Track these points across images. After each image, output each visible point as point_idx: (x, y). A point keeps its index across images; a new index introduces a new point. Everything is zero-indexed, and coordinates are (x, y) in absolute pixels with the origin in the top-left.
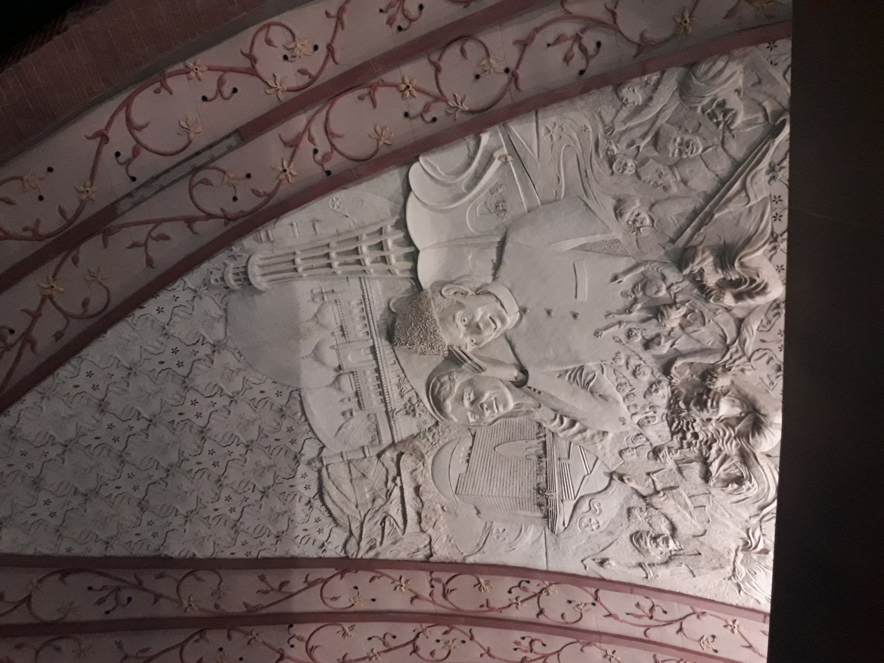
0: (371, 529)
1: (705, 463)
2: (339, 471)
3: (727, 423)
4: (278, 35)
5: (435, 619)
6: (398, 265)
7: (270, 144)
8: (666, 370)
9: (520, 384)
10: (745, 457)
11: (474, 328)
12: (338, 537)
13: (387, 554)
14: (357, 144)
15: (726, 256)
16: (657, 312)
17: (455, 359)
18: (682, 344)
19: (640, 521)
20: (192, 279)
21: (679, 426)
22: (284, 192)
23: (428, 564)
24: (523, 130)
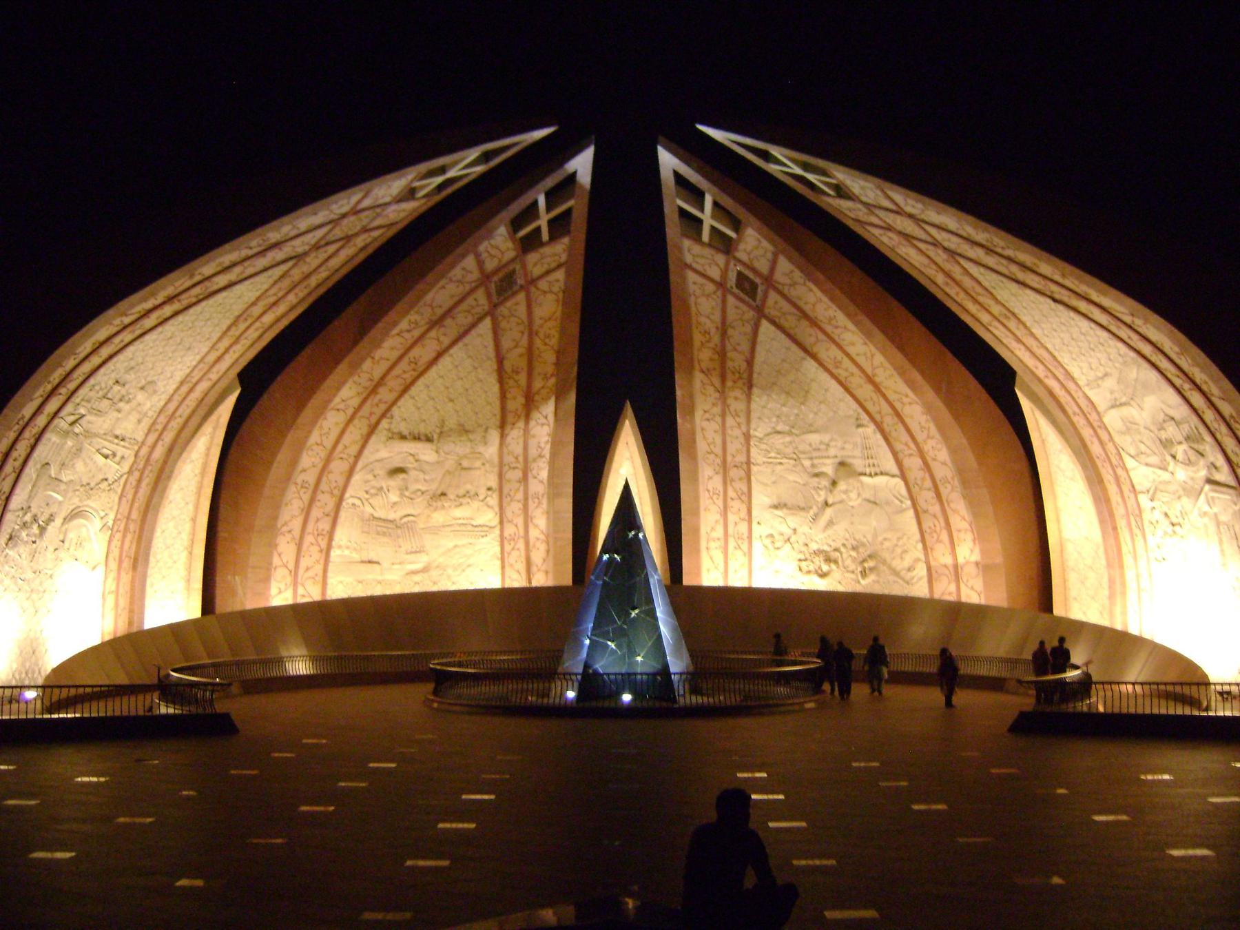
0: (764, 447)
1: (806, 560)
2: (788, 439)
3: (820, 567)
4: (939, 446)
5: (724, 461)
6: (868, 471)
7: (905, 437)
8: (836, 550)
9: (826, 504)
10: (809, 572)
11: (846, 492)
12: (761, 435)
13: (753, 451)
14: (907, 462)
15: (871, 569)
16: (854, 548)
17: (834, 483)
18: (845, 556)
19: (777, 537)
20: (860, 410)
21: (817, 553)
22: (892, 440)
23: (748, 463)
24: (911, 513)
